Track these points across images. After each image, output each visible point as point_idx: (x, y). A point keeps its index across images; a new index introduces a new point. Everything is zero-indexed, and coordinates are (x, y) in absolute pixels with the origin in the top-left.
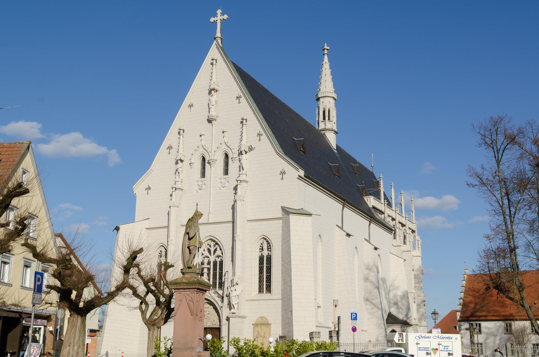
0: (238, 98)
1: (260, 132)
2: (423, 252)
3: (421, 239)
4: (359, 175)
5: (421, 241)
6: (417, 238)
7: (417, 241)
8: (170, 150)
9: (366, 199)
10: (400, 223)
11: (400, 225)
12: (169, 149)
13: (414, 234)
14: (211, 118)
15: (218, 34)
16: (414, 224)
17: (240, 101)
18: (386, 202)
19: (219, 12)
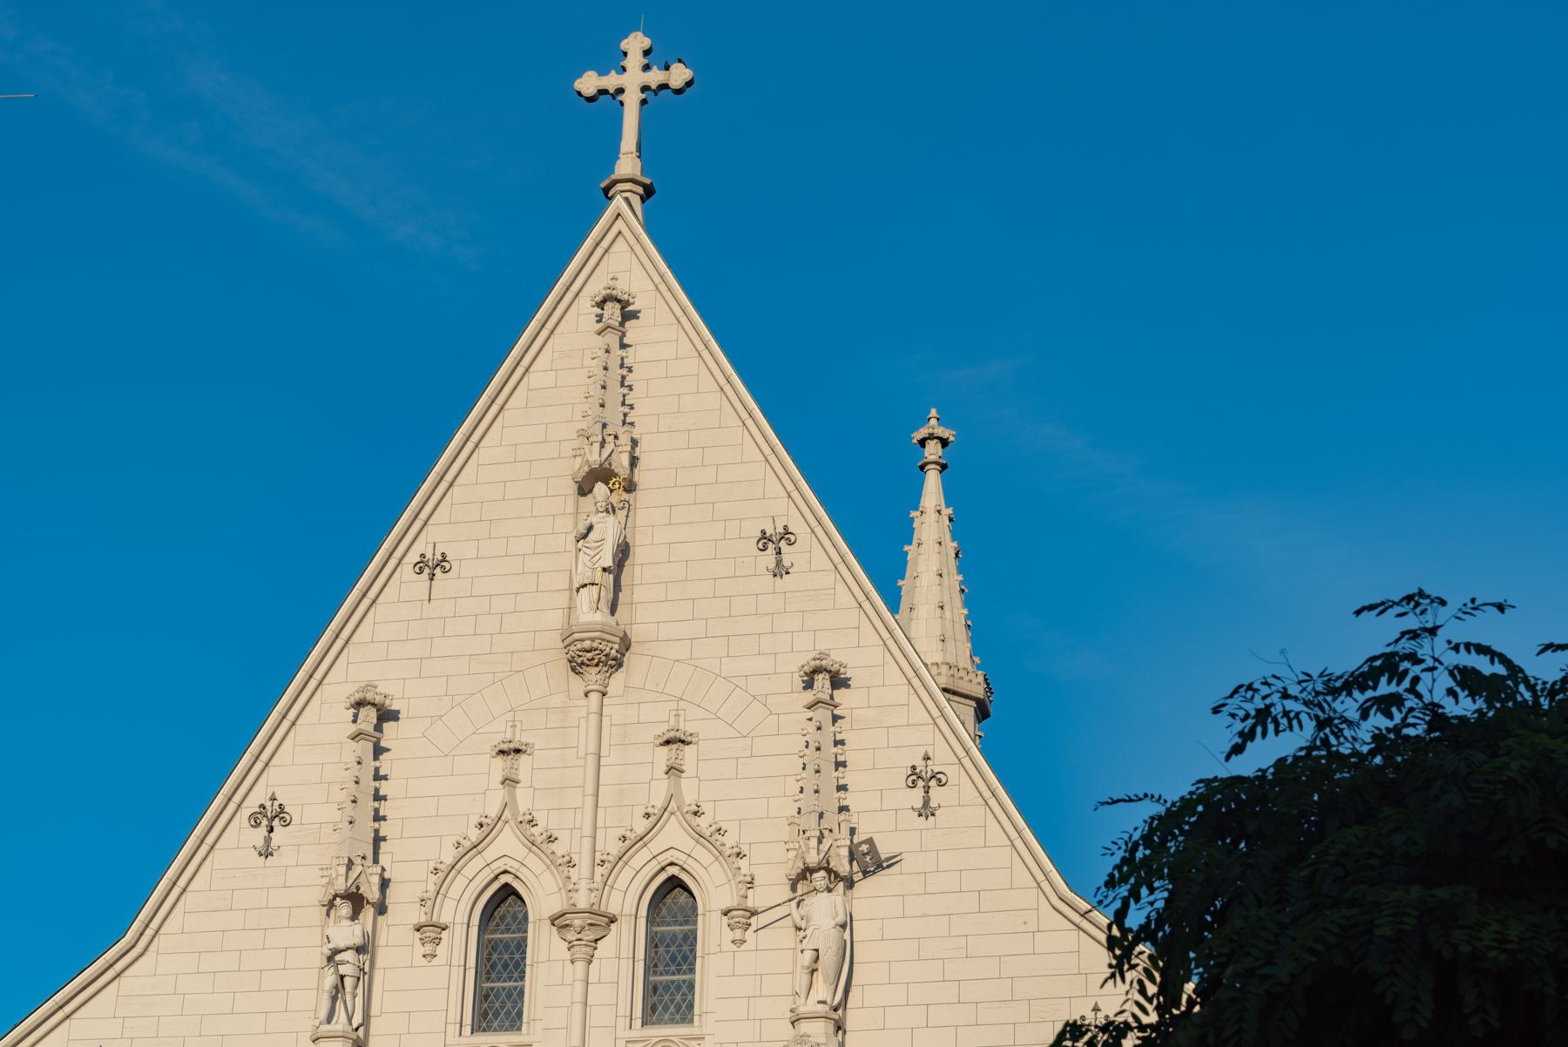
0: (773, 541)
1: (927, 758)
8: (271, 830)
12: (265, 822)
14: (587, 644)
15: (628, 164)
17: (786, 563)
19: (635, 44)
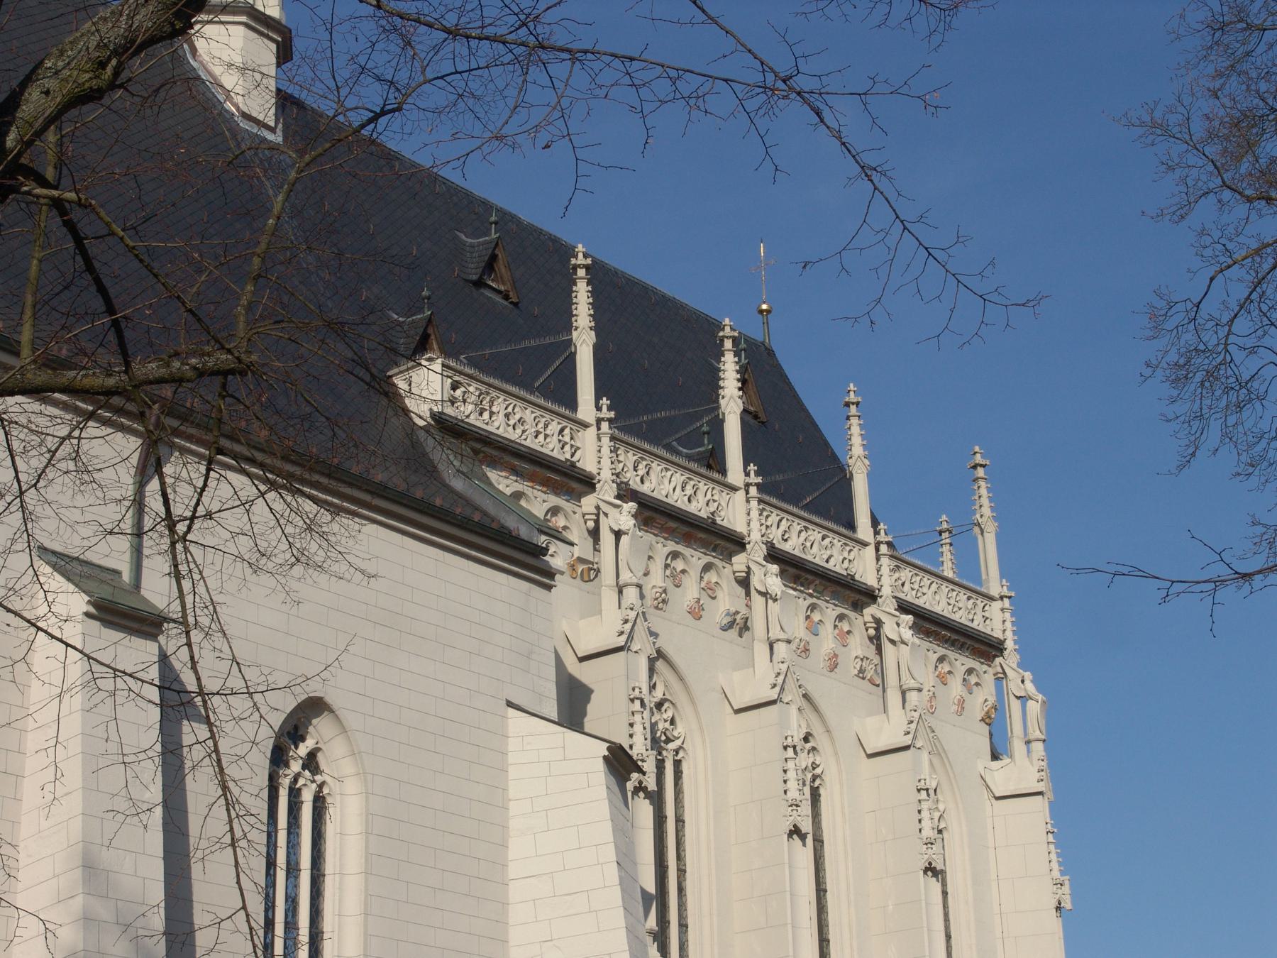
2: (1057, 766)
3: (1039, 690)
4: (506, 297)
5: (1040, 697)
6: (1014, 686)
7: (1015, 705)
9: (401, 383)
10: (774, 555)
11: (775, 568)
13: (998, 660)
16: (992, 599)
18: (605, 413)
